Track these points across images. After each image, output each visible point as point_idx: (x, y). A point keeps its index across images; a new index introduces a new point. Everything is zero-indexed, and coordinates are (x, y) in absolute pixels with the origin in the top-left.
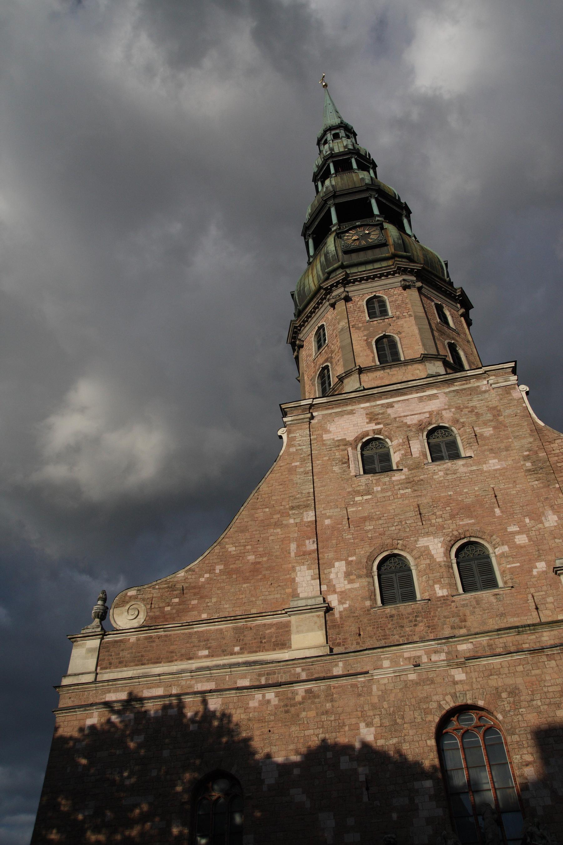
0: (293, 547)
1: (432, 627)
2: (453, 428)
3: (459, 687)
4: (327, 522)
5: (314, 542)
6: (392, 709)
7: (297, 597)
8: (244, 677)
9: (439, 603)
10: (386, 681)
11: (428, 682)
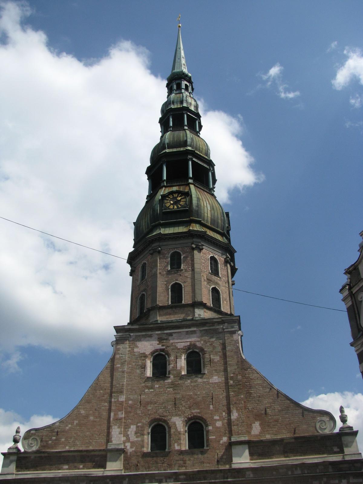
4: (130, 402)
9: (175, 453)
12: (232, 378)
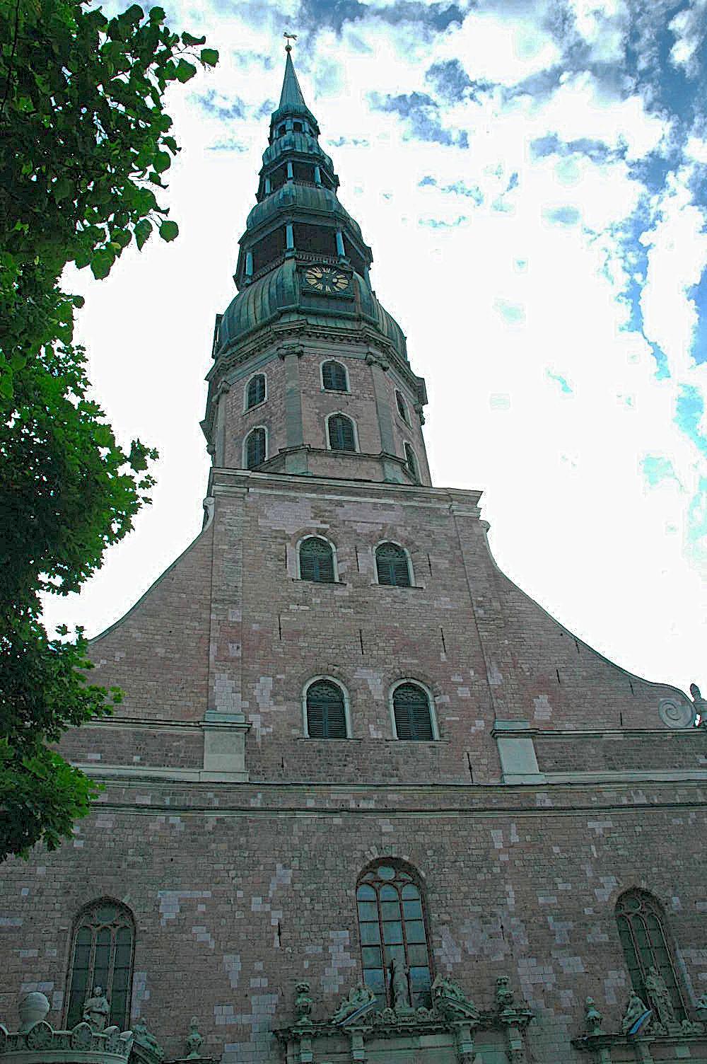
0: (213, 647)
2: (405, 549)
3: (385, 839)
4: (255, 627)
5: (238, 648)
6: (312, 853)
7: (213, 709)
8: (143, 793)
9: (372, 745)
10: (309, 822)
11: (354, 830)
12: (480, 605)
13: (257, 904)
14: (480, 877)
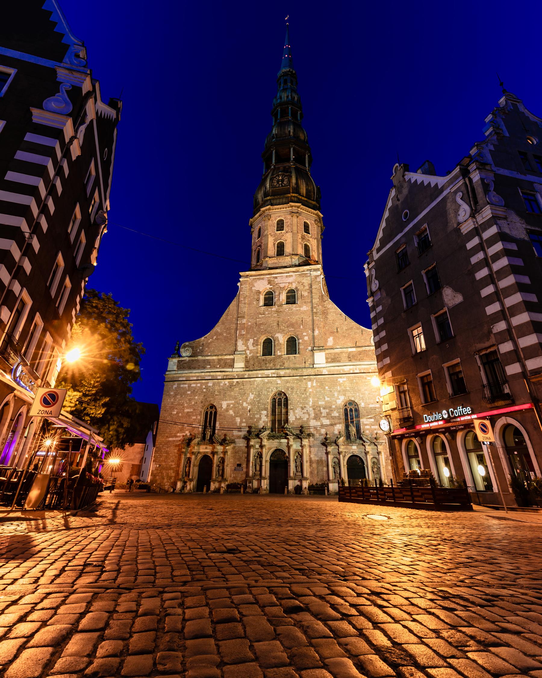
1: (274, 365)
13: (245, 404)
14: (303, 396)
